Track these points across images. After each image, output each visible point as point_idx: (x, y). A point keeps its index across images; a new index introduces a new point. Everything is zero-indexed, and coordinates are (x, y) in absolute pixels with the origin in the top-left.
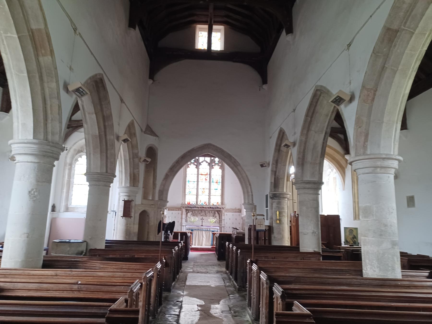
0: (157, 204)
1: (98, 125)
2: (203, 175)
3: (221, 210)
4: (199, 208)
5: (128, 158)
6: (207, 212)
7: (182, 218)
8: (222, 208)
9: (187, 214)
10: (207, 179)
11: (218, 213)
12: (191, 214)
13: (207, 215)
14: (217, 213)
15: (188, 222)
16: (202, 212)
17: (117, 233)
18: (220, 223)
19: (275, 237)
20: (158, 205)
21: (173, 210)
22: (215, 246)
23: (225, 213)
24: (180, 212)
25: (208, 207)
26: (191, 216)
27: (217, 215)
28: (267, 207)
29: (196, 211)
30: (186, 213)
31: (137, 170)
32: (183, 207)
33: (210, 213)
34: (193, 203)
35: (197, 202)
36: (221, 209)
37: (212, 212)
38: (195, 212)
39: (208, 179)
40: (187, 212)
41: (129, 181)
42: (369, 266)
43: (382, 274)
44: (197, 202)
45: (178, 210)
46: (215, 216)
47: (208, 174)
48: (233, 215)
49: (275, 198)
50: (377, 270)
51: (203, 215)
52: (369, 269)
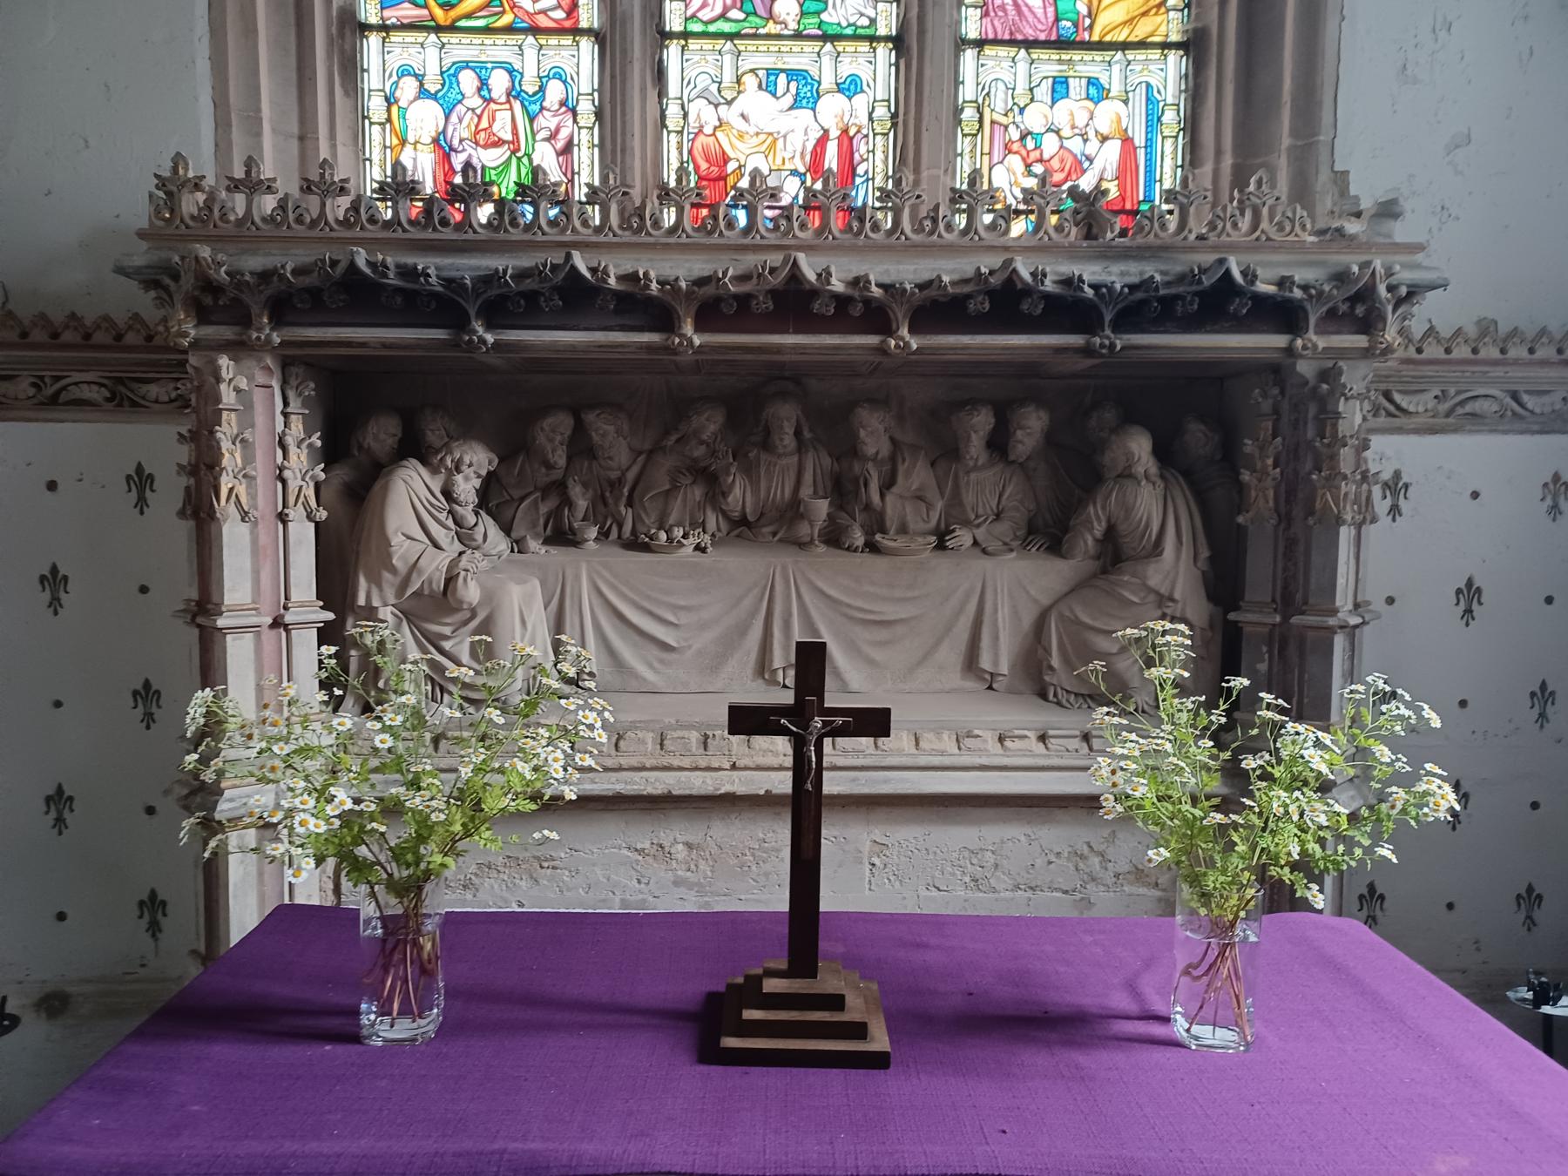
3: (1276, 371)
8: (1334, 320)
12: (467, 487)
13: (893, 507)
14: (1140, 446)
16: (766, 445)
25: (950, 271)
26: (464, 536)
29: (607, 431)
33: (947, 453)
37: (998, 444)
38: (582, 447)
40: (381, 433)
46: (1088, 540)
51: (793, 511)
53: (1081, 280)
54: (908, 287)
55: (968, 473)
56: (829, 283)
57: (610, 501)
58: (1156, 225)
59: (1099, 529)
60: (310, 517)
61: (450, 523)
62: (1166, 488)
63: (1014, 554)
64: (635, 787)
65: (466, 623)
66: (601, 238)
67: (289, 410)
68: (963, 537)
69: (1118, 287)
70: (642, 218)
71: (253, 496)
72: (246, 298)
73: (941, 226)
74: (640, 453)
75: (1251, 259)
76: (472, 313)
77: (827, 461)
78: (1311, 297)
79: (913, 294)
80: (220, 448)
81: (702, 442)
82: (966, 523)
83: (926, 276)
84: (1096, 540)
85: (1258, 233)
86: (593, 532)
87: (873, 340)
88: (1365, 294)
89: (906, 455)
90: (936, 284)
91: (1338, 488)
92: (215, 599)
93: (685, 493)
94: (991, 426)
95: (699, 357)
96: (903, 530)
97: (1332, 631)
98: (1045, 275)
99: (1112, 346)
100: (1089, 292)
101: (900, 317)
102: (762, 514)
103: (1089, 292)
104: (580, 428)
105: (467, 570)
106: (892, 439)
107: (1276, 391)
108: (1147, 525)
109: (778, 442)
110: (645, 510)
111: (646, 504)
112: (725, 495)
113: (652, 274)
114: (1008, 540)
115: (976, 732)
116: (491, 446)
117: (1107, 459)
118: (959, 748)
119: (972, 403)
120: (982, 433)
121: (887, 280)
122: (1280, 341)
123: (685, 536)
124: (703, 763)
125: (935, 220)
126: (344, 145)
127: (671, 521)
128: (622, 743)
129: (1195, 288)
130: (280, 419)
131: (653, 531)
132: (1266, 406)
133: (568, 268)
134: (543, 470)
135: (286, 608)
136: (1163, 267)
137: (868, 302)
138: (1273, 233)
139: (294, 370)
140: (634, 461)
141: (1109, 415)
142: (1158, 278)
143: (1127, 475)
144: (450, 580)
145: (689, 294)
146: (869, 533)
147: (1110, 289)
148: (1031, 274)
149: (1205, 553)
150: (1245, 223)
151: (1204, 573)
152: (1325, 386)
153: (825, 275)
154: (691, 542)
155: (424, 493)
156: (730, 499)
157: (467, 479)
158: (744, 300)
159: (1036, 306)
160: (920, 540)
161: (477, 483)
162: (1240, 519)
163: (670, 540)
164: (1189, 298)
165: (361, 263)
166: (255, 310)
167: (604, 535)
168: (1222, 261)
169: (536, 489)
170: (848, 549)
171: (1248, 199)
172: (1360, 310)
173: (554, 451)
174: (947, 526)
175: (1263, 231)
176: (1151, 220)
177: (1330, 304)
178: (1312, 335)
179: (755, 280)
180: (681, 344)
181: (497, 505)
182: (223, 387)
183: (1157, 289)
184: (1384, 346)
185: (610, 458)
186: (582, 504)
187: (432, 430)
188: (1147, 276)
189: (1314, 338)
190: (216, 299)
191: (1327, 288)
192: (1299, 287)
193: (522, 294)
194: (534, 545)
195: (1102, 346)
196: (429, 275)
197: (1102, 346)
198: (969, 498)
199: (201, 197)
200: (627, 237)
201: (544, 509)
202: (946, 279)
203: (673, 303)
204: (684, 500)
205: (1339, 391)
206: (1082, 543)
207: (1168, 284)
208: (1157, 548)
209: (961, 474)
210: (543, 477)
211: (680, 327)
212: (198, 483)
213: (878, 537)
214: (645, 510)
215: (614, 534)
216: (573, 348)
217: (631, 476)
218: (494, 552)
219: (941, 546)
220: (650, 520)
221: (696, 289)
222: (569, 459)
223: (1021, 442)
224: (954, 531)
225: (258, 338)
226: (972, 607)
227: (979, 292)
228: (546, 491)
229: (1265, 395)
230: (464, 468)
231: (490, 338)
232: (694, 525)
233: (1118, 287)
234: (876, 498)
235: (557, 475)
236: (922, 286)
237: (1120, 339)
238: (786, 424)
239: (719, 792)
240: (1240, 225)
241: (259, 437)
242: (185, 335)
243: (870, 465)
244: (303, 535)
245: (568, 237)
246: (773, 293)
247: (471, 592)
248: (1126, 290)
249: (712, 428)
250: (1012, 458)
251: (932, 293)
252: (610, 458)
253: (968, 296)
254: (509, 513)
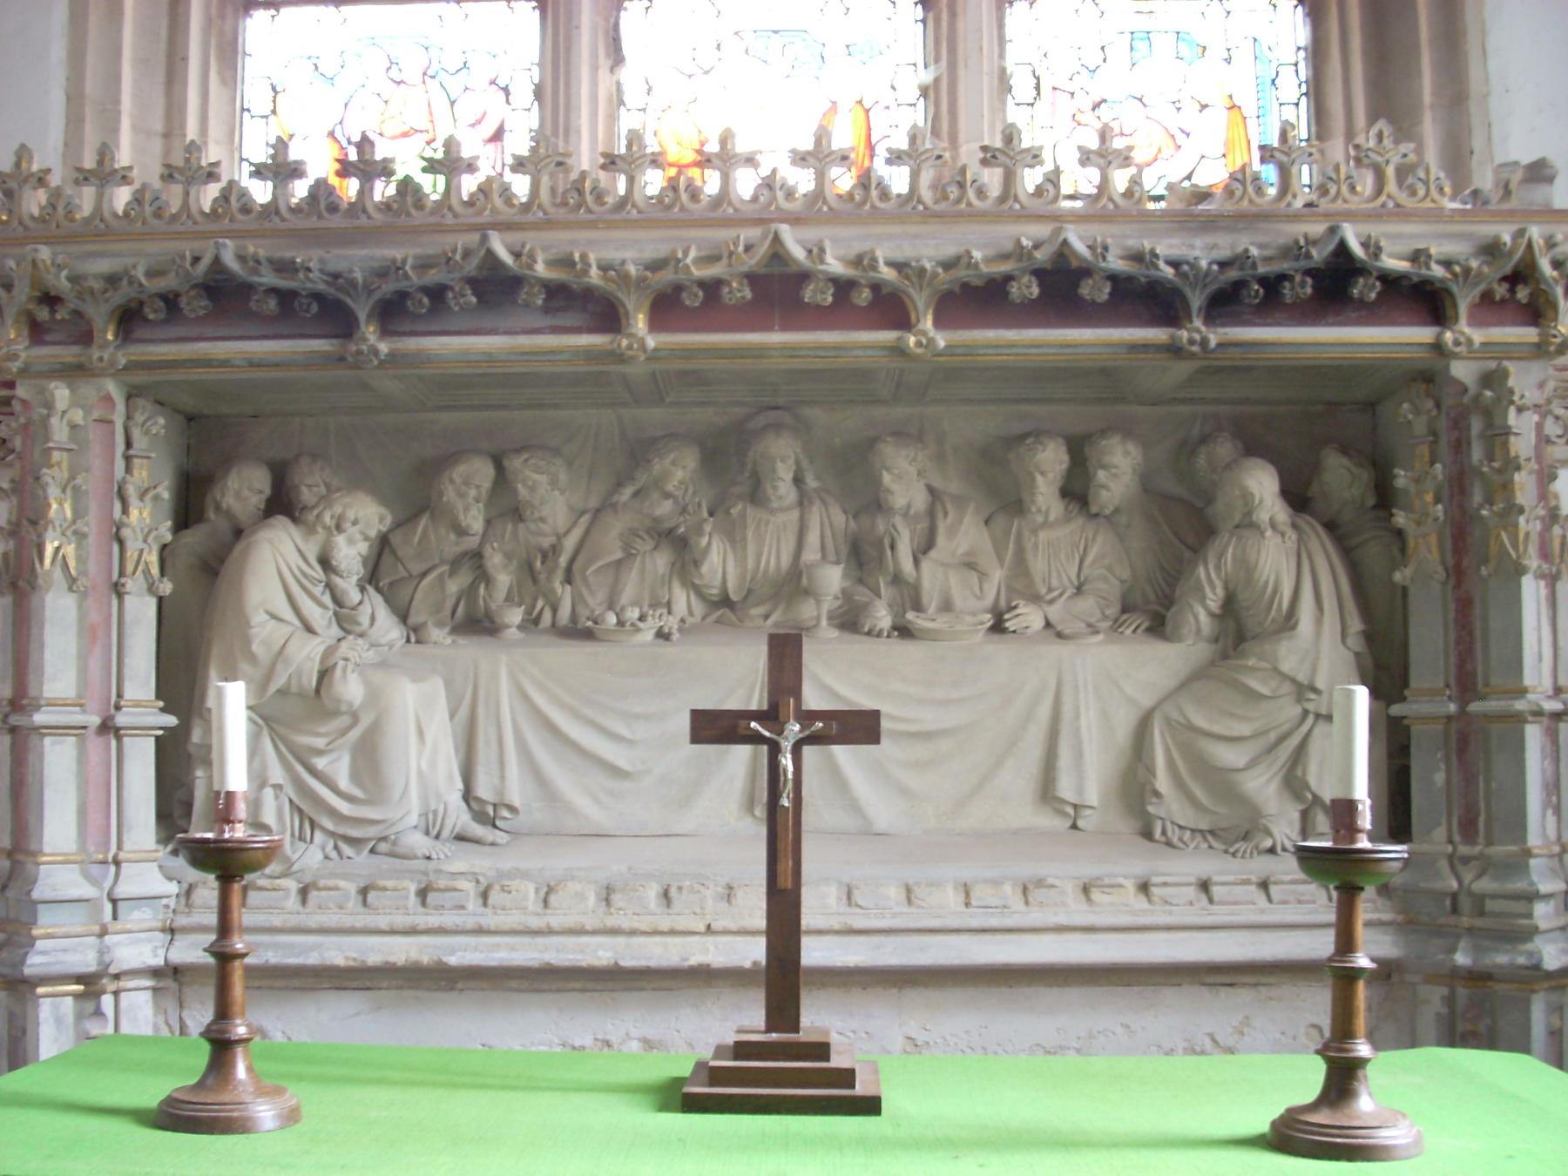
4: (608, 316)
8: (1489, 307)
12: (351, 553)
13: (931, 577)
16: (756, 496)
26: (345, 619)
36: (1468, 332)
37: (1076, 492)
46: (1200, 615)
53: (1155, 255)
54: (928, 266)
55: (1035, 531)
56: (822, 261)
57: (542, 577)
58: (1250, 189)
59: (1214, 599)
60: (151, 589)
61: (327, 599)
62: (1300, 540)
63: (1100, 637)
64: (571, 957)
65: (344, 732)
66: (530, 217)
67: (131, 452)
68: (1029, 617)
69: (1204, 264)
70: (580, 192)
71: (80, 559)
72: (90, 310)
73: (971, 194)
74: (583, 513)
75: (1374, 230)
76: (362, 316)
77: (839, 518)
78: (1455, 275)
79: (935, 275)
80: (46, 498)
81: (667, 495)
82: (1035, 599)
83: (950, 251)
84: (1212, 615)
85: (1383, 198)
86: (515, 616)
87: (887, 336)
88: (1522, 274)
89: (949, 507)
90: (965, 260)
91: (1516, 526)
92: (32, 692)
93: (643, 562)
94: (1065, 466)
95: (657, 366)
96: (947, 606)
97: (1519, 719)
98: (1106, 248)
99: (1204, 342)
100: (1169, 272)
101: (920, 304)
102: (750, 591)
103: (1169, 272)
104: (502, 478)
105: (346, 660)
106: (931, 490)
107: (1429, 404)
108: (1275, 591)
109: (770, 491)
110: (588, 586)
111: (591, 579)
112: (697, 564)
113: (592, 257)
114: (1093, 620)
115: (1051, 881)
116: (383, 500)
117: (1220, 507)
118: (1027, 903)
119: (1037, 435)
120: (1051, 475)
121: (899, 256)
122: (1423, 334)
123: (642, 618)
124: (664, 925)
125: (961, 185)
126: (217, 143)
127: (624, 599)
128: (553, 899)
129: (1303, 264)
130: (120, 464)
131: (597, 612)
132: (1420, 426)
133: (483, 252)
134: (452, 537)
135: (118, 708)
136: (1262, 239)
137: (876, 287)
138: (1403, 198)
139: (140, 402)
140: (575, 523)
141: (1224, 449)
142: (1254, 251)
143: (1248, 524)
144: (325, 674)
145: (641, 281)
146: (898, 610)
147: (1194, 265)
148: (1089, 247)
149: (1356, 625)
150: (1366, 183)
151: (1357, 654)
152: (1488, 393)
153: (815, 251)
154: (651, 625)
155: (295, 560)
156: (705, 569)
157: (351, 541)
158: (712, 288)
159: (1100, 290)
160: (969, 619)
161: (363, 547)
162: (1398, 577)
163: (621, 623)
164: (1298, 278)
165: (229, 260)
166: (98, 324)
167: (531, 622)
168: (1333, 230)
169: (442, 562)
170: (869, 633)
171: (1367, 156)
172: (1522, 294)
173: (466, 509)
174: (1009, 602)
175: (1389, 196)
176: (1243, 182)
177: (1482, 287)
178: (1464, 326)
179: (725, 261)
180: (630, 347)
181: (391, 584)
182: (54, 421)
183: (1254, 266)
184: (1558, 340)
185: (542, 520)
186: (504, 581)
187: (309, 486)
188: (1240, 249)
189: (1467, 330)
190: (53, 312)
191: (1474, 264)
192: (1439, 262)
193: (426, 290)
194: (438, 634)
195: (1191, 342)
196: (309, 270)
197: (1191, 342)
198: (1038, 565)
199: (42, 196)
200: (561, 214)
201: (454, 587)
202: (977, 255)
203: (619, 294)
204: (642, 571)
205: (1505, 397)
206: (1191, 618)
207: (1267, 260)
208: (1289, 621)
209: (1026, 533)
210: (452, 546)
211: (629, 325)
212: (19, 551)
213: (910, 615)
214: (588, 586)
215: (547, 617)
216: (489, 357)
217: (570, 543)
218: (384, 641)
219: (998, 627)
220: (595, 601)
221: (649, 274)
222: (488, 522)
223: (1105, 487)
224: (1015, 607)
225: (101, 359)
226: (1044, 712)
227: (1023, 271)
228: (455, 564)
229: (1417, 411)
230: (347, 525)
231: (384, 347)
232: (654, 605)
233: (1204, 264)
234: (907, 565)
235: (471, 543)
236: (949, 265)
237: (1215, 333)
238: (779, 465)
239: (687, 964)
240: (1359, 188)
241: (91, 482)
242: (13, 357)
243: (898, 520)
244: (142, 613)
245: (486, 217)
246: (752, 278)
247: (351, 689)
248: (1215, 267)
249: (679, 474)
250: (1094, 509)
251: (962, 273)
252: (542, 520)
253: (1009, 278)
254: (404, 593)
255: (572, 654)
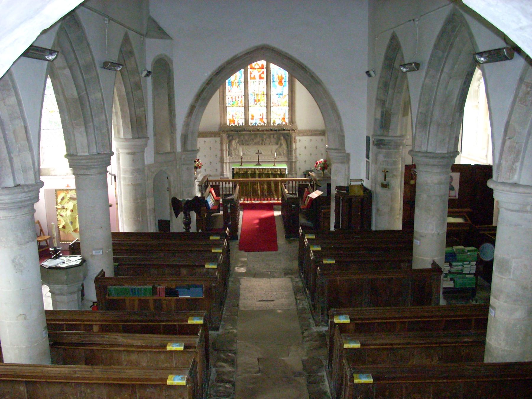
0: (181, 159)
1: (75, 84)
2: (255, 69)
5: (124, 93)
6: (265, 137)
7: (222, 150)
8: (292, 131)
9: (230, 142)
10: (262, 76)
11: (284, 137)
13: (266, 142)
14: (282, 138)
15: (233, 156)
16: (257, 137)
17: (122, 212)
18: (289, 155)
19: (378, 210)
20: (182, 159)
21: (206, 137)
22: (280, 202)
23: (298, 138)
24: (218, 139)
26: (237, 144)
27: (283, 141)
28: (368, 157)
30: (227, 141)
31: (143, 109)
32: (223, 131)
34: (241, 124)
35: (246, 121)
36: (291, 132)
37: (273, 137)
38: (244, 138)
39: (264, 76)
40: (231, 138)
41: (130, 130)
42: (493, 337)
43: (508, 349)
44: (246, 121)
45: (215, 136)
46: (279, 144)
47: (265, 67)
48: (311, 140)
49: (382, 146)
50: (503, 343)
51: (259, 142)
52: (493, 340)
68: (271, 144)
244: (227, 145)
255: (248, 146)
